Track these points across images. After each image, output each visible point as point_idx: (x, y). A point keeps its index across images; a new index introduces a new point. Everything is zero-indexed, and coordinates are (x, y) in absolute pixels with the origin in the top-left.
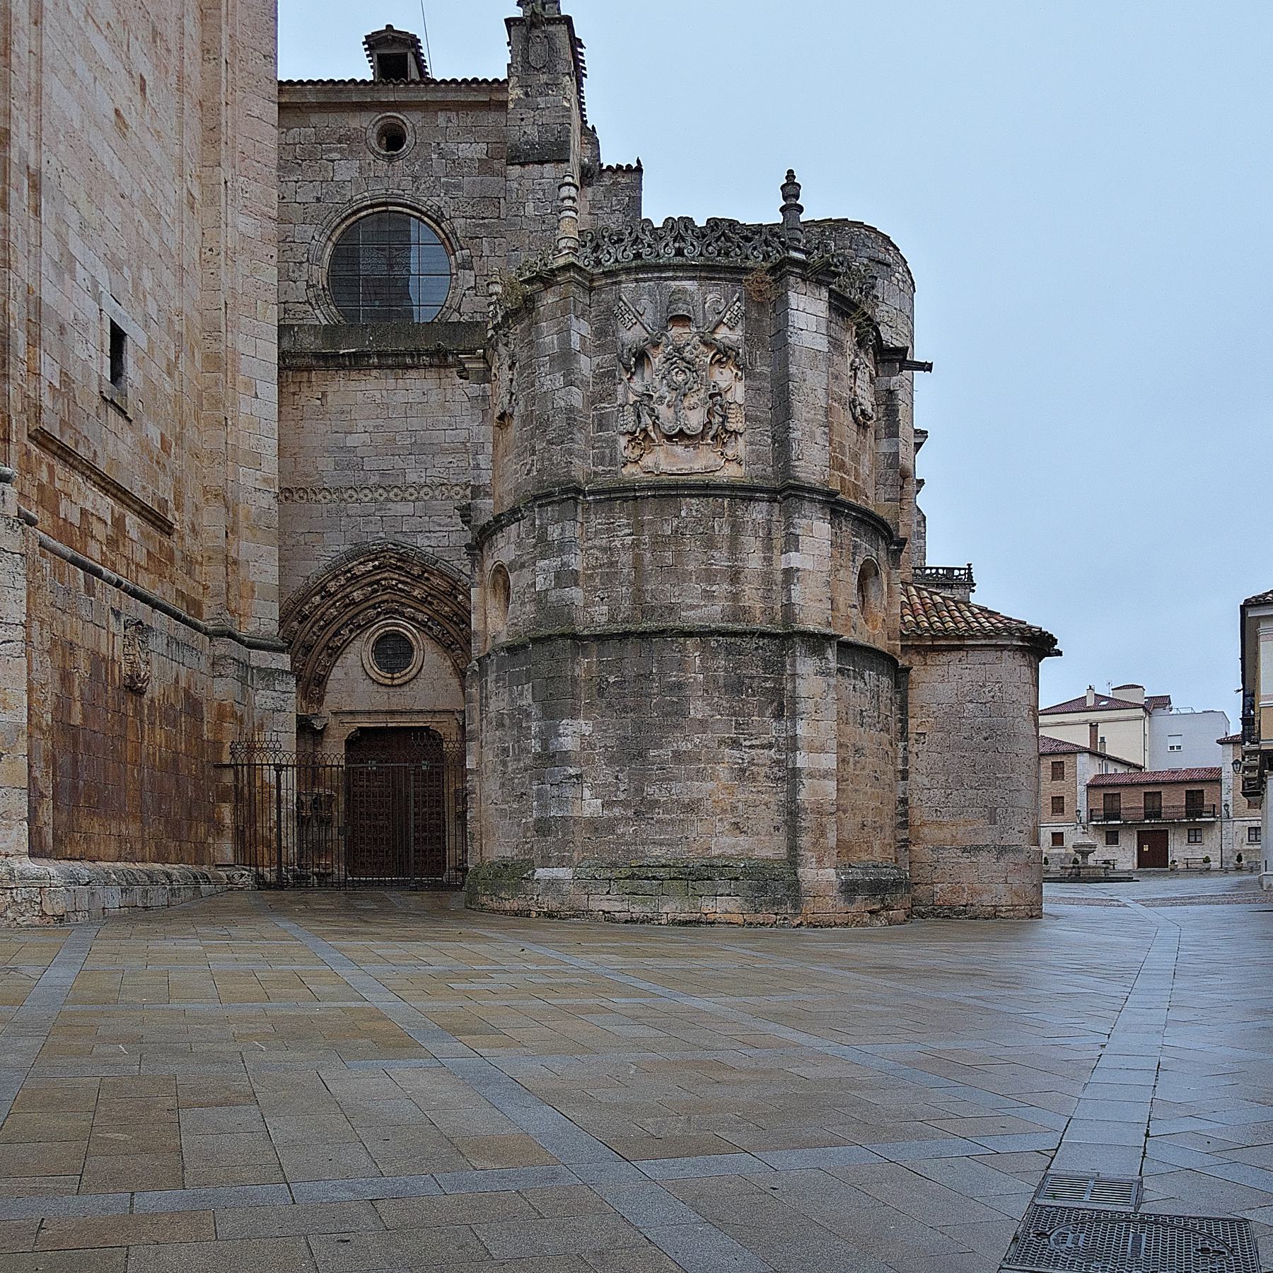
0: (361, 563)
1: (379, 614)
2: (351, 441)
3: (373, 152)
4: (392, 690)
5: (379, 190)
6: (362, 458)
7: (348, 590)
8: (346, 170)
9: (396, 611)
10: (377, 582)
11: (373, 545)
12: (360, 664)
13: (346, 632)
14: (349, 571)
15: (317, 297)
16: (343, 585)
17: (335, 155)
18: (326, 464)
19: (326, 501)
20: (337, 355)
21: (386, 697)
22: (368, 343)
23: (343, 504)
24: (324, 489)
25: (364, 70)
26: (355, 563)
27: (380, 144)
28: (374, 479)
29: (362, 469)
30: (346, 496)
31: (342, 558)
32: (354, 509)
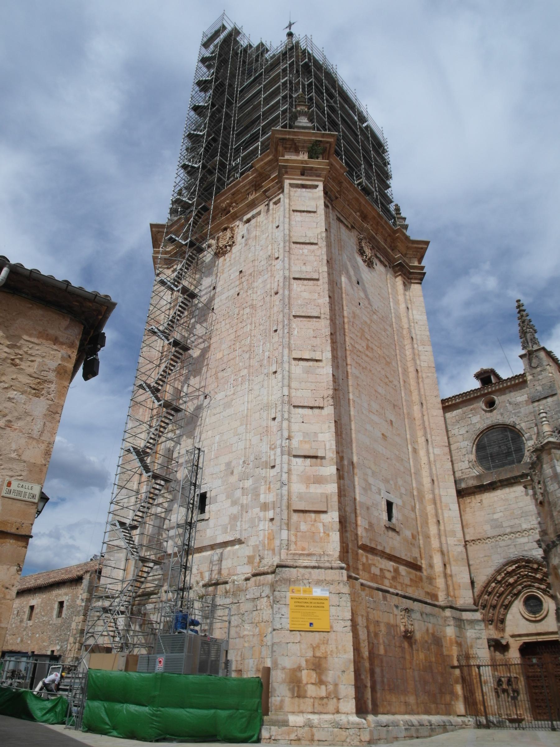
1: (523, 588)
2: (496, 516)
3: (484, 410)
5: (489, 422)
7: (507, 579)
8: (475, 419)
9: (530, 586)
10: (519, 573)
14: (505, 570)
15: (473, 465)
17: (470, 416)
18: (487, 527)
20: (482, 486)
22: (494, 478)
23: (497, 542)
25: (477, 384)
27: (486, 407)
28: (508, 530)
32: (502, 543)
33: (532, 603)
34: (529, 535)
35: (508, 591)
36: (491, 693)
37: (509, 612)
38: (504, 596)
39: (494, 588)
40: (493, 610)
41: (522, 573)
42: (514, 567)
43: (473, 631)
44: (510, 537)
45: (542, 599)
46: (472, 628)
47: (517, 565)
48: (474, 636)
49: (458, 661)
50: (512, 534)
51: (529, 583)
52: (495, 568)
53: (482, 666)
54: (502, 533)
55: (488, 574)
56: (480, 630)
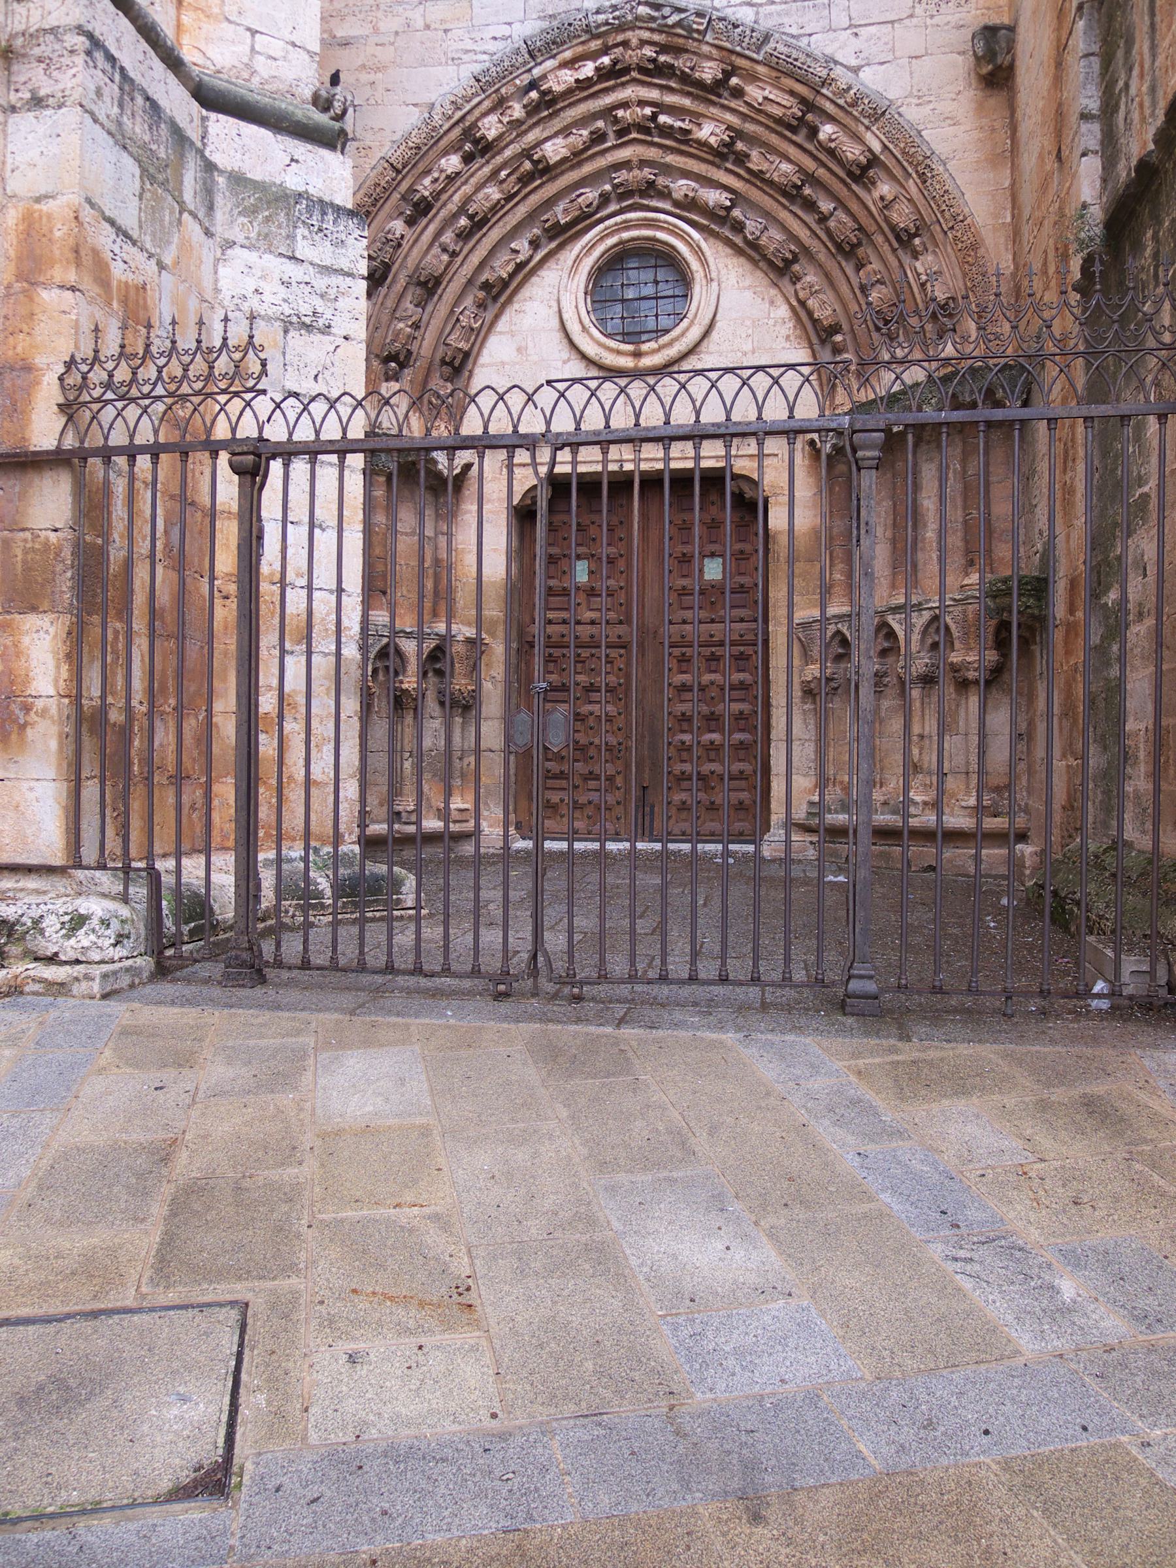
0: (565, 65)
1: (605, 199)
7: (531, 137)
10: (608, 113)
11: (598, 12)
12: (555, 323)
13: (522, 245)
14: (533, 85)
16: (518, 123)
26: (550, 64)
31: (517, 52)
35: (522, 211)
37: (501, 325)
38: (495, 234)
39: (451, 179)
40: (421, 304)
41: (620, 113)
42: (588, 70)
45: (695, 265)
46: (264, 243)
47: (606, 60)
48: (273, 300)
49: (69, 409)
51: (647, 173)
52: (477, 68)
55: (433, 97)
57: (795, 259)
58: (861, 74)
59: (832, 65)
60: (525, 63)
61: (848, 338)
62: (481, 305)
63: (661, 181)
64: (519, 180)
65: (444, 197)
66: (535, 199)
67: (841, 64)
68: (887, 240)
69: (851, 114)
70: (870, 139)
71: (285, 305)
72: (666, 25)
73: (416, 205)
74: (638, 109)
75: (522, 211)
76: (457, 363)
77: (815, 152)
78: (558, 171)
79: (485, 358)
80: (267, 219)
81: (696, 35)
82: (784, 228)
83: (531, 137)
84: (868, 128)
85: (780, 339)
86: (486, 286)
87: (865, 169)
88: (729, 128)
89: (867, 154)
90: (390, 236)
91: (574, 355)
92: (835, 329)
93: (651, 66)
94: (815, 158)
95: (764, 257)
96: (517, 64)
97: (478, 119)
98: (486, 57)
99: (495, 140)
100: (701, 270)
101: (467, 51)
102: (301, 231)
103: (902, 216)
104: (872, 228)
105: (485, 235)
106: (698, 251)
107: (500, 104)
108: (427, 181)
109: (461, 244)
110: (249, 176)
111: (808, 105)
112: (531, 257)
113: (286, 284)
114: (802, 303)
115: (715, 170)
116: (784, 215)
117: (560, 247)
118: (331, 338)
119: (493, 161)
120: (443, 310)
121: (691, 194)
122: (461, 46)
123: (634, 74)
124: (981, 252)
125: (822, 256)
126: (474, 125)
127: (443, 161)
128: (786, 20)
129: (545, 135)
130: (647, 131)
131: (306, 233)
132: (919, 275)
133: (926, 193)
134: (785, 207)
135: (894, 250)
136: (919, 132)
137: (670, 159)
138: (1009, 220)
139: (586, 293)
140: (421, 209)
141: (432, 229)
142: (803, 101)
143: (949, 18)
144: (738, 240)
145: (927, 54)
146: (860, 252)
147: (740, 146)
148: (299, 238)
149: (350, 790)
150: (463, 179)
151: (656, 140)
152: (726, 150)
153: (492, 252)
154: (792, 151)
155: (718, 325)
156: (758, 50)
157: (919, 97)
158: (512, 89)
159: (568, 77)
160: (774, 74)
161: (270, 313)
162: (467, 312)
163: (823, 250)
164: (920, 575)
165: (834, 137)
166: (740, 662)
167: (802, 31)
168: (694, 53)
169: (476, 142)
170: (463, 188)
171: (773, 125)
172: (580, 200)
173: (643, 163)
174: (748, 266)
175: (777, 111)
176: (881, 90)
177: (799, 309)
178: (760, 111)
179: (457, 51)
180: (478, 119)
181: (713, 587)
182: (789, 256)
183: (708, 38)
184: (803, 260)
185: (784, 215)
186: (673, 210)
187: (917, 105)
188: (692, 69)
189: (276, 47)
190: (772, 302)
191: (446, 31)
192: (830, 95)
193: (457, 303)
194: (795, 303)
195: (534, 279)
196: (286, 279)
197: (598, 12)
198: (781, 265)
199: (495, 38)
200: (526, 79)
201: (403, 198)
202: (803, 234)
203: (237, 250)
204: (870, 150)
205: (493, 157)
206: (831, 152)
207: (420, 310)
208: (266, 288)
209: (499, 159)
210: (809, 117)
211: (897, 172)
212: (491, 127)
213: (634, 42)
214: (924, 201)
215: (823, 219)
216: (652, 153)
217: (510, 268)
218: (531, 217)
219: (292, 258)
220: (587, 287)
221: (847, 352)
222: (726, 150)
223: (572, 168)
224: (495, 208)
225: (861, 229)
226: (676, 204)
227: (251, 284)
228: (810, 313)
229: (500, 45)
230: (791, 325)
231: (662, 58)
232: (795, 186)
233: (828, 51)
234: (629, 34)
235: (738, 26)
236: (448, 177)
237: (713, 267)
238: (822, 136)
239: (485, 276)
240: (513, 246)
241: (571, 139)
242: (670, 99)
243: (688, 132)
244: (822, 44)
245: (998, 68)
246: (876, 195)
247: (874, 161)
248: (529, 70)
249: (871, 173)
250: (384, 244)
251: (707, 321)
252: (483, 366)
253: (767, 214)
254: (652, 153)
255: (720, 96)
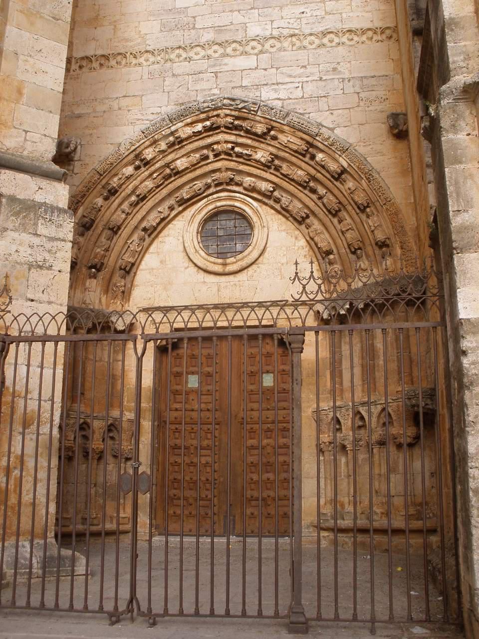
0: (187, 125)
4: (223, 279)
6: (194, 17)
7: (170, 158)
10: (208, 146)
12: (181, 248)
13: (164, 208)
14: (172, 133)
16: (163, 151)
19: (148, 63)
21: (215, 289)
23: (169, 64)
24: (147, 52)
26: (180, 125)
29: (194, 28)
30: (173, 56)
31: (163, 120)
32: (181, 67)
33: (227, 224)
34: (261, 52)
35: (165, 192)
36: (43, 462)
37: (152, 249)
38: (150, 204)
39: (128, 178)
41: (215, 147)
42: (199, 127)
43: (26, 237)
44: (210, 52)
45: (255, 219)
46: (23, 228)
47: (208, 123)
48: (25, 254)
50: (216, 47)
51: (229, 174)
52: (143, 127)
53: (18, 340)
54: (187, 42)
56: (51, 239)
57: (308, 217)
58: (335, 131)
59: (320, 127)
60: (167, 125)
61: (337, 256)
62: (142, 239)
63: (238, 178)
64: (164, 178)
65: (124, 186)
66: (171, 187)
67: (325, 127)
68: (354, 209)
69: (331, 149)
70: (341, 159)
71: (30, 257)
72: (237, 108)
73: (109, 191)
74: (225, 145)
75: (165, 192)
76: (128, 269)
77: (314, 166)
78: (184, 173)
79: (143, 265)
80: (24, 217)
81: (253, 112)
82: (300, 201)
83: (170, 158)
84: (340, 156)
85: (301, 256)
86: (145, 230)
87: (340, 175)
88: (271, 154)
89: (341, 168)
90: (95, 206)
91: (191, 264)
92: (329, 253)
93: (231, 126)
94: (315, 169)
95: (291, 215)
96: (163, 125)
97: (143, 150)
98: (148, 122)
99: (151, 160)
100: (259, 221)
101: (138, 120)
102: (41, 221)
103: (360, 198)
104: (345, 202)
105: (145, 204)
106: (256, 212)
107: (155, 142)
108: (115, 179)
109: (132, 208)
110: (18, 197)
111: (311, 145)
112: (169, 215)
113: (31, 247)
114: (312, 239)
115: (265, 173)
116: (300, 195)
117: (184, 210)
118: (53, 272)
119: (150, 169)
120: (121, 242)
121: (252, 185)
122: (136, 117)
123: (223, 129)
124: (400, 216)
125: (321, 215)
126: (141, 153)
127: (124, 169)
128: (297, 107)
129: (177, 157)
130: (230, 155)
131: (43, 222)
132: (370, 226)
133: (371, 187)
134: (302, 192)
135: (357, 214)
136: (365, 159)
137: (242, 167)
138: (412, 201)
139: (197, 233)
140: (113, 192)
141: (117, 202)
142: (308, 142)
143: (377, 107)
144: (278, 207)
145: (367, 123)
146: (340, 214)
147: (277, 162)
148: (40, 224)
149: (52, 508)
150: (134, 178)
151: (234, 159)
152: (270, 164)
153: (148, 213)
154: (303, 165)
155: (268, 249)
156: (284, 119)
157: (364, 143)
158: (161, 136)
159: (189, 131)
160: (293, 130)
161: (22, 261)
162: (134, 243)
163: (322, 212)
164: (377, 384)
165: (323, 159)
166: (284, 433)
167: (305, 112)
168: (252, 120)
169: (142, 160)
170: (134, 182)
171: (293, 153)
172: (195, 187)
173: (227, 169)
174: (284, 219)
175: (295, 148)
176: (345, 139)
177: (311, 242)
178: (286, 147)
179: (134, 119)
180: (143, 150)
181: (268, 390)
182: (305, 216)
183: (259, 113)
184: (312, 218)
185: (300, 195)
186: (244, 192)
187: (365, 146)
188: (251, 127)
189: (36, 137)
190: (296, 238)
191: (129, 111)
192: (321, 140)
193: (128, 239)
194: (308, 239)
195: (170, 226)
196: (31, 244)
197: (204, 102)
198: (300, 219)
199: (153, 114)
200: (168, 131)
201: (103, 187)
202: (311, 204)
203: (9, 232)
204: (342, 166)
205: (150, 167)
206: (323, 167)
207: (109, 242)
208: (21, 249)
209: (153, 168)
210: (311, 150)
211: (356, 176)
212: (149, 154)
213: (222, 115)
214: (370, 191)
215: (320, 198)
216: (232, 165)
217: (158, 220)
218: (169, 195)
219: (36, 234)
220: (198, 230)
221: (337, 264)
222: (270, 164)
223: (191, 172)
224: (150, 192)
225: (340, 203)
226: (245, 189)
227: (14, 248)
228: (316, 244)
229: (155, 116)
230: (307, 250)
231: (236, 122)
232: (305, 182)
233: (319, 121)
234: (219, 112)
235: (273, 109)
236: (126, 177)
237: (264, 220)
238: (317, 159)
239: (144, 224)
240: (159, 209)
241: (190, 158)
242: (240, 140)
243: (250, 155)
244: (315, 117)
245: (401, 132)
246: (347, 187)
247: (344, 171)
248: (170, 127)
249: (343, 176)
250: (92, 210)
251: (262, 248)
252: (142, 270)
253: (292, 195)
254: (232, 165)
255: (266, 139)
